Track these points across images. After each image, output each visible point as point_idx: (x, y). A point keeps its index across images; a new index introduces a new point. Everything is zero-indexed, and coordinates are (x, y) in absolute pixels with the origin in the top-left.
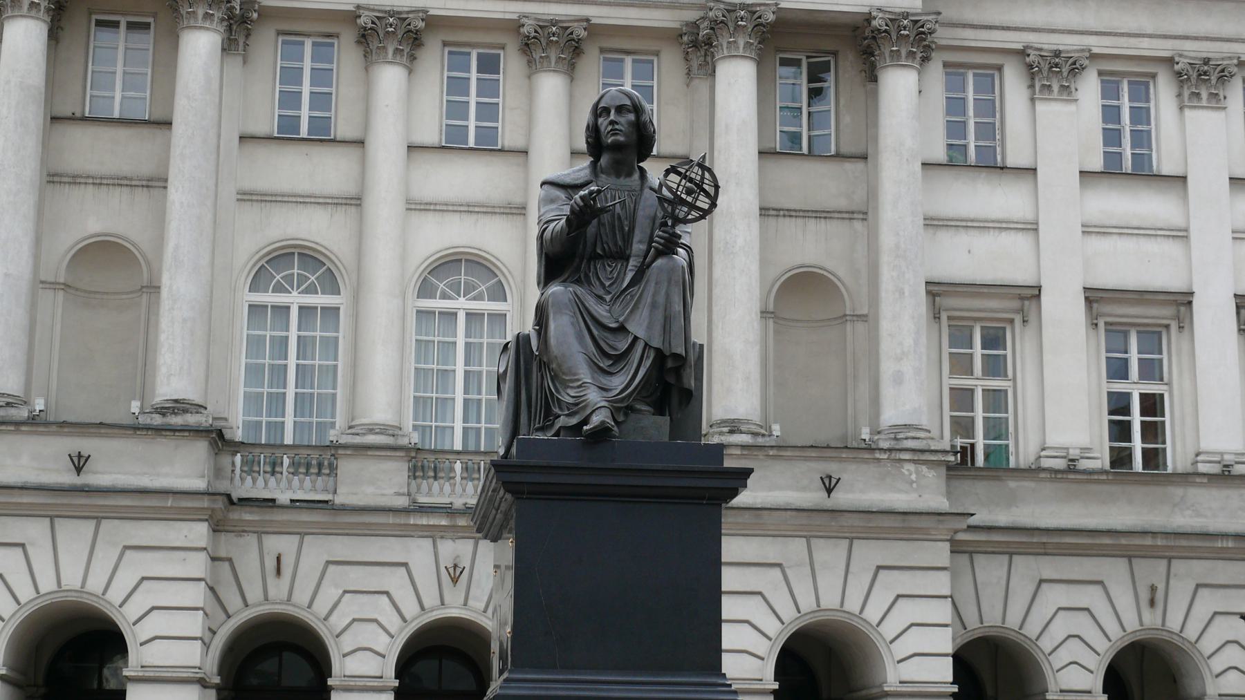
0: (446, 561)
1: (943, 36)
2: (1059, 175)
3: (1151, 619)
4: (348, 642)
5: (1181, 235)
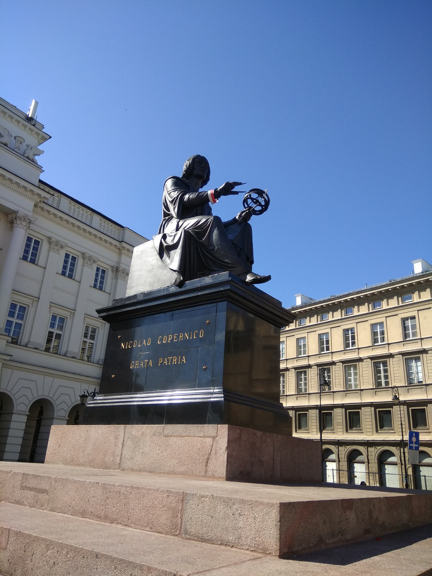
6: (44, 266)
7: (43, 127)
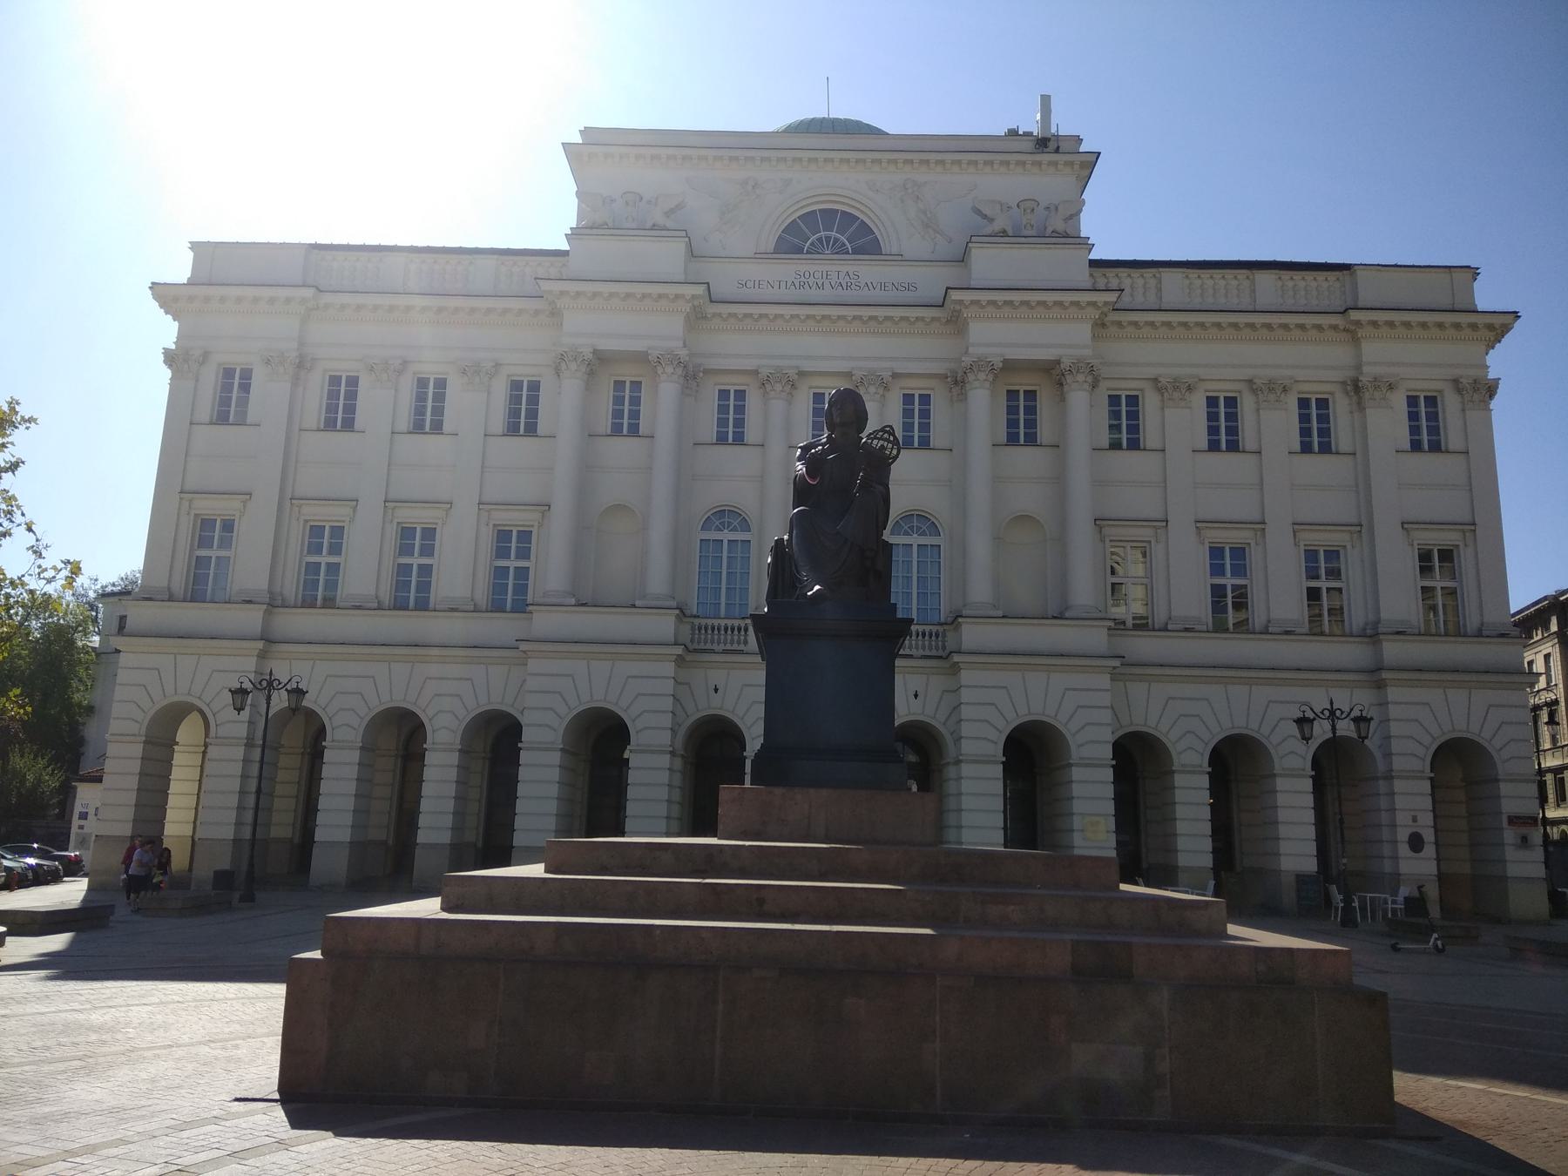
6: (1159, 446)
7: (1079, 140)
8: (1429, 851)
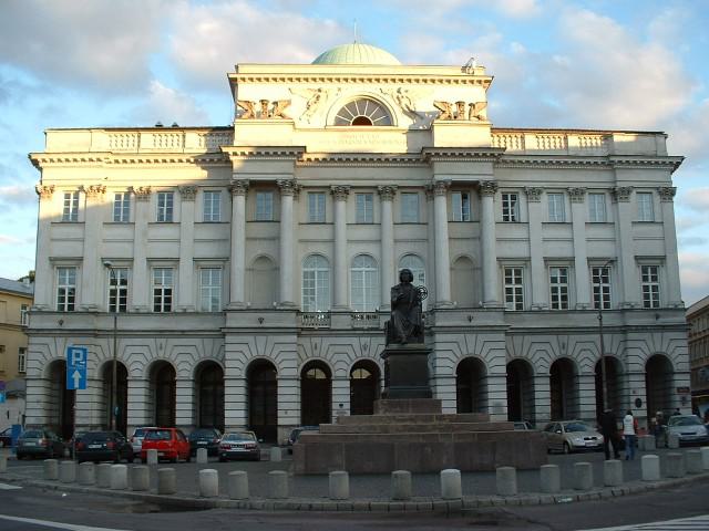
0: (363, 343)
1: (500, 184)
2: (535, 225)
3: (563, 352)
4: (337, 367)
5: (572, 240)
8: (644, 406)
